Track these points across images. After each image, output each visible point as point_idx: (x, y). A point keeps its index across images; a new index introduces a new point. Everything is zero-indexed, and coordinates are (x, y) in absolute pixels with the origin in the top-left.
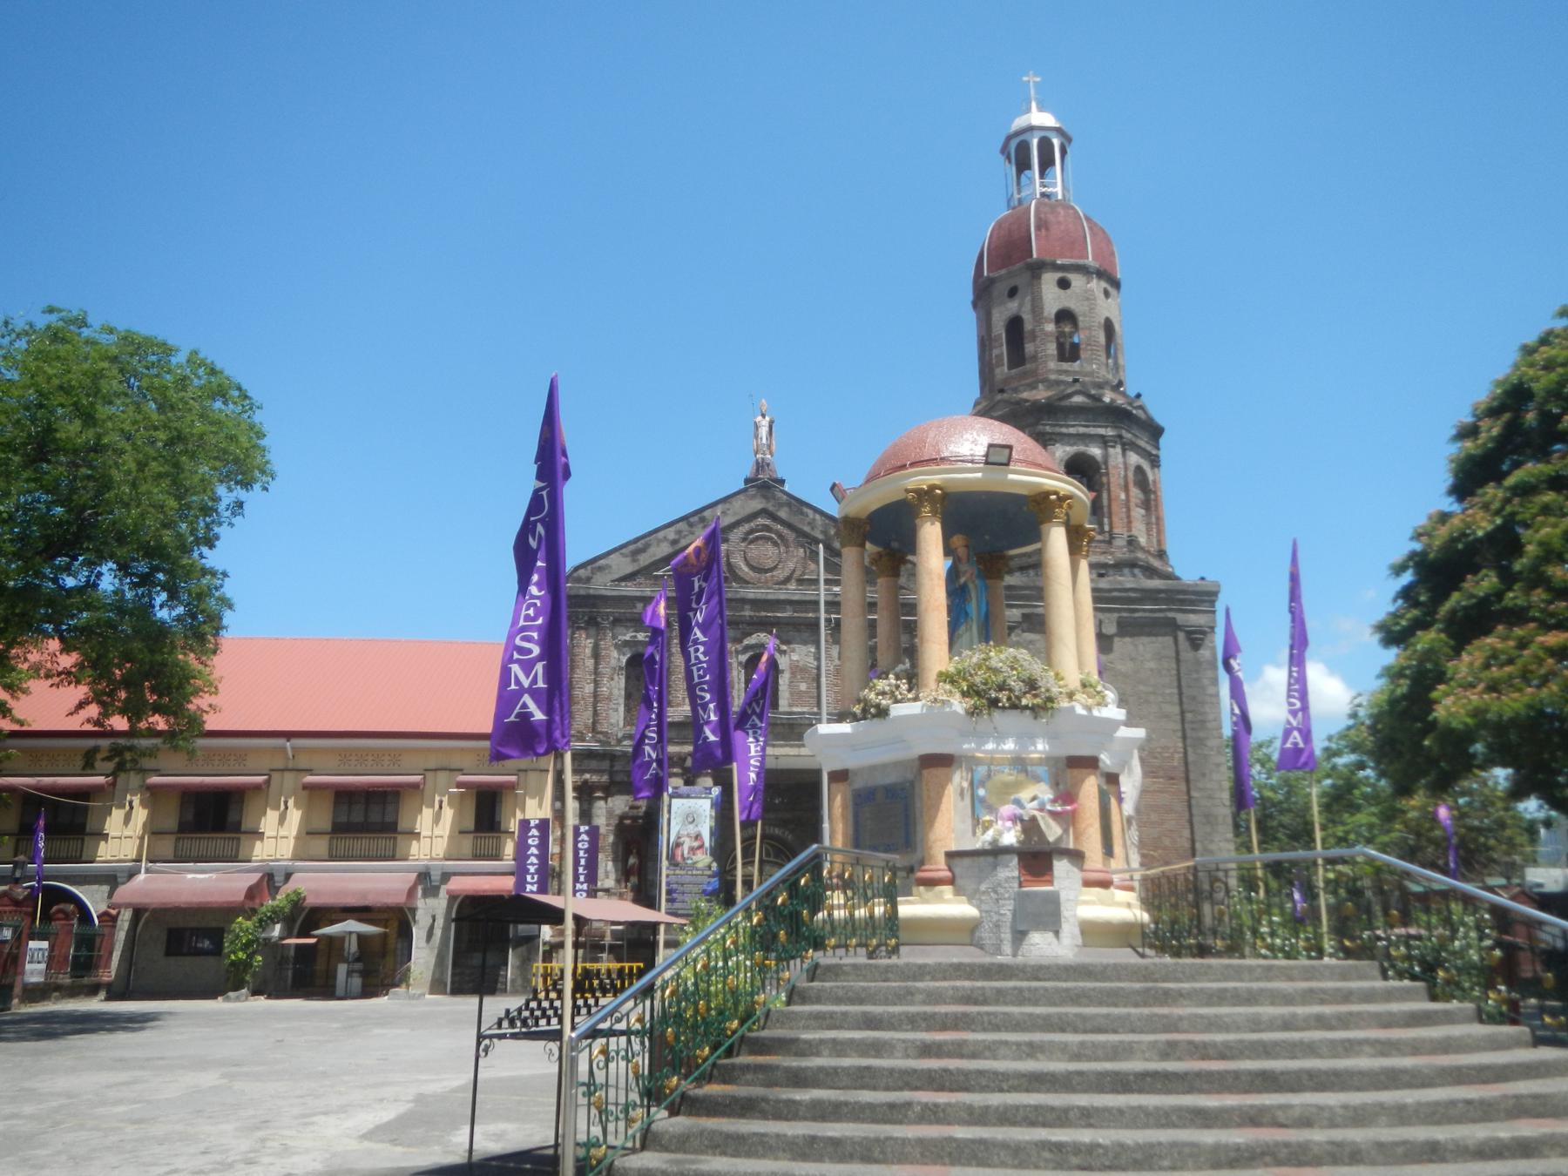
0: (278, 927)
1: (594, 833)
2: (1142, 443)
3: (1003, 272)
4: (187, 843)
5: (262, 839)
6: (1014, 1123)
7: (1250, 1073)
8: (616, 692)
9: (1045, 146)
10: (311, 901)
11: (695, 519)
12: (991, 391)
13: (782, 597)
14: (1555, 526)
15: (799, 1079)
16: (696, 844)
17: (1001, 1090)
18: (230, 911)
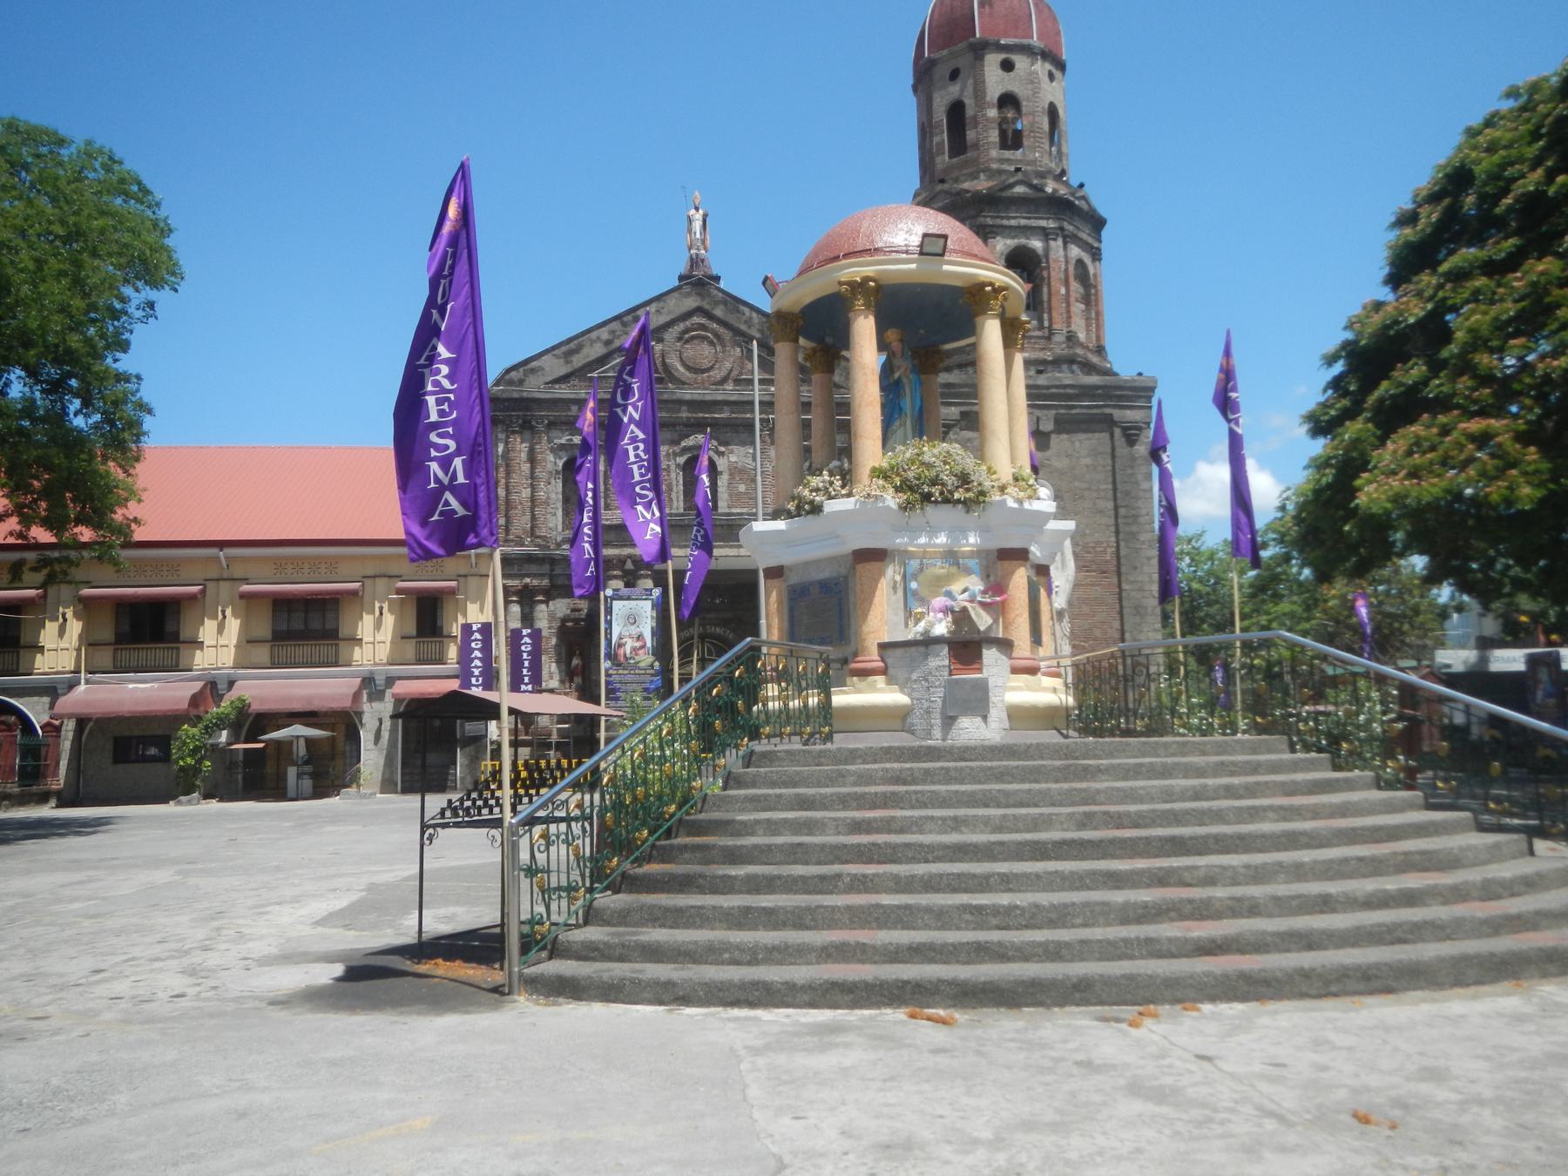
0: (225, 733)
1: (536, 635)
2: (1084, 236)
3: (945, 52)
5: (202, 649)
6: (938, 891)
7: (1160, 839)
8: (553, 496)
10: (256, 707)
11: (630, 318)
12: (932, 181)
13: (719, 398)
14: (1485, 313)
15: (733, 856)
16: (638, 644)
17: (927, 861)
18: (174, 719)
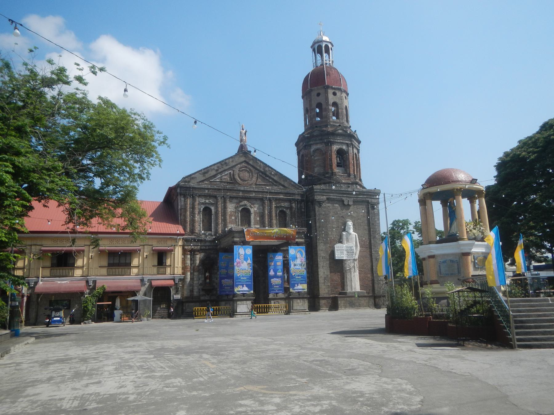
4: (55, 271)
9: (327, 47)
10: (107, 289)
13: (252, 190)
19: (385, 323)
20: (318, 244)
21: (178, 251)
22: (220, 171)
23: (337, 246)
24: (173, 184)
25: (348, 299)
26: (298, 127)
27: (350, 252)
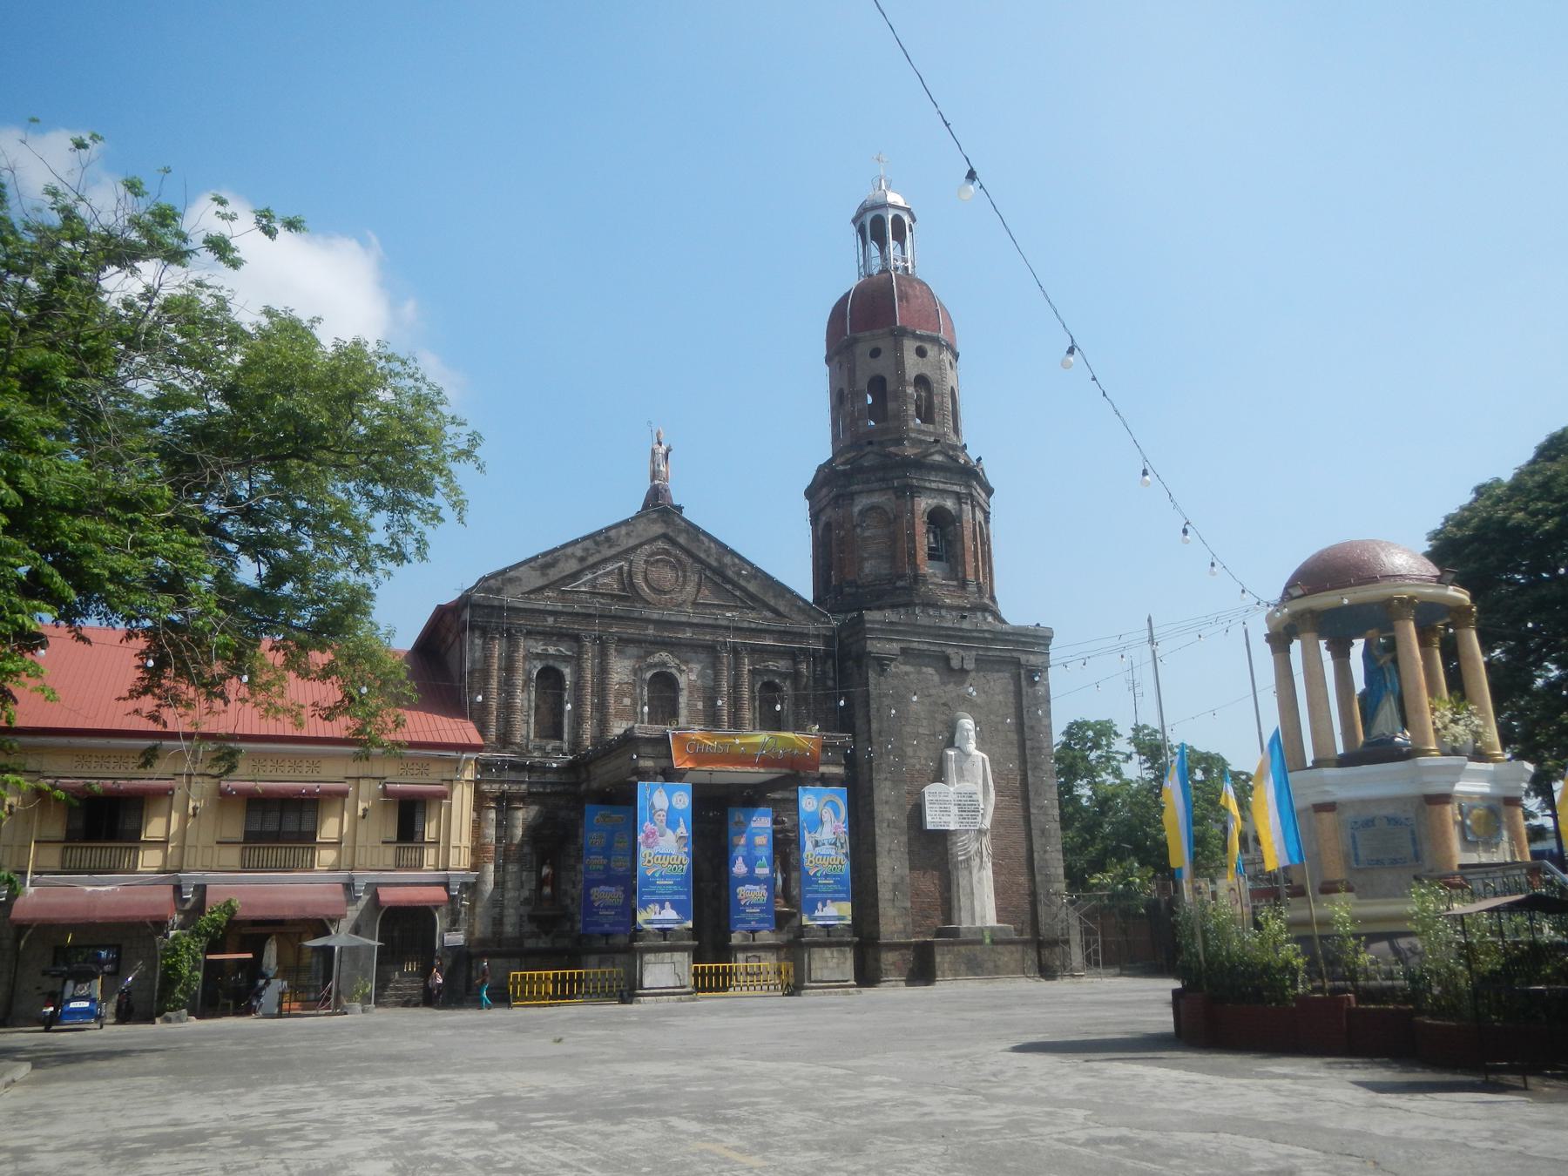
9: (898, 221)
10: (241, 913)
13: (684, 619)
19: (1171, 1019)
20: (875, 783)
21: (462, 799)
22: (591, 561)
23: (932, 791)
24: (449, 596)
25: (963, 949)
26: (815, 445)
27: (968, 808)
